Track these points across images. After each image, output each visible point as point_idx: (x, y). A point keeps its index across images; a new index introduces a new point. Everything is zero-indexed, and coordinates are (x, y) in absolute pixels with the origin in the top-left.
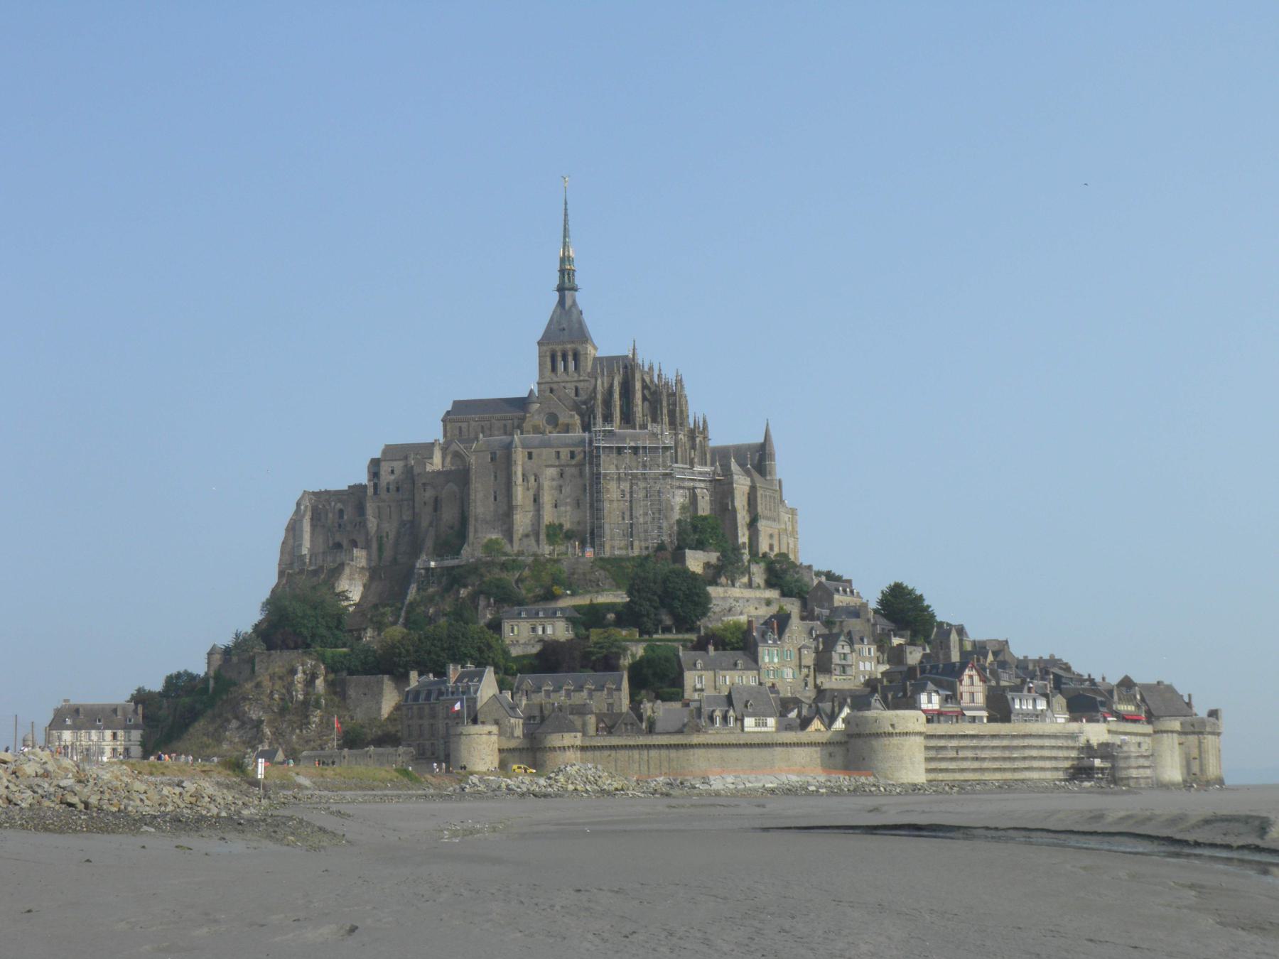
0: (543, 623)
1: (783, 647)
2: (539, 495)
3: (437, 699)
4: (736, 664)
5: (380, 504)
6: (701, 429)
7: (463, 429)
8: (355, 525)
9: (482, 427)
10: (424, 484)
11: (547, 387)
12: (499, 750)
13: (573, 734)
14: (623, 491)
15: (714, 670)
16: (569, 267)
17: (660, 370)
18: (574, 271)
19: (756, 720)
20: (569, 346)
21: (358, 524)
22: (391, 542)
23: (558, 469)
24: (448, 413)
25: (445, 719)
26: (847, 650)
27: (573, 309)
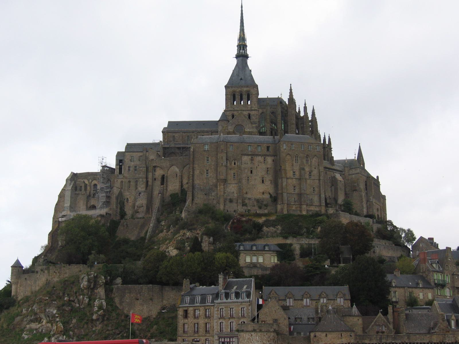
0: (256, 254)
2: (237, 173)
3: (213, 302)
4: (418, 284)
5: (123, 180)
6: (327, 143)
10: (155, 167)
13: (349, 333)
14: (294, 172)
15: (404, 287)
16: (244, 43)
17: (305, 104)
18: (246, 46)
22: (130, 204)
23: (250, 157)
24: (164, 128)
25: (219, 319)
27: (246, 68)
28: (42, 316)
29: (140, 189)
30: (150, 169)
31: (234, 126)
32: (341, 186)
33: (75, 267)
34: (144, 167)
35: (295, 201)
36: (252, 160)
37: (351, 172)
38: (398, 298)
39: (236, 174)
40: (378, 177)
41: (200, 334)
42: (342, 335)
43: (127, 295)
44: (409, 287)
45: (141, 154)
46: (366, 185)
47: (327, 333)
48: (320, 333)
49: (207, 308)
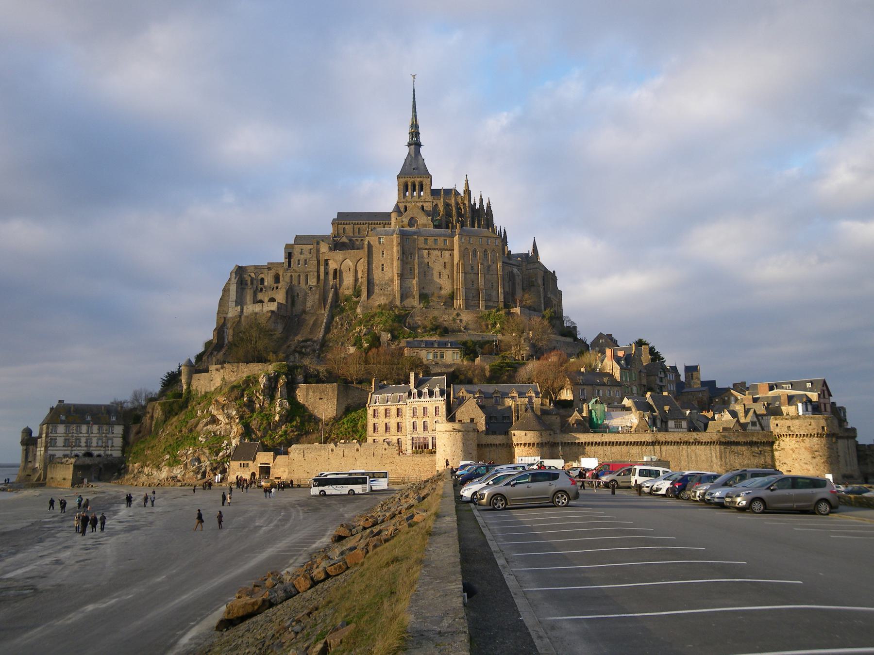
1: (631, 370)
7: (346, 229)
8: (274, 288)
9: (359, 228)
11: (402, 205)
12: (479, 446)
13: (548, 432)
15: (592, 385)
16: (416, 131)
17: (481, 196)
18: (419, 133)
19: (675, 422)
20: (418, 179)
21: (275, 288)
23: (427, 251)
26: (662, 375)
27: (419, 157)
28: (220, 417)
29: (310, 283)
30: (322, 262)
31: (409, 218)
32: (518, 280)
33: (254, 365)
34: (314, 261)
35: (473, 297)
36: (429, 254)
37: (529, 267)
38: (586, 396)
39: (412, 269)
40: (554, 272)
41: (392, 433)
42: (542, 434)
43: (311, 394)
44: (597, 385)
45: (312, 246)
46: (543, 280)
47: (527, 432)
48: (519, 432)
49: (399, 407)
